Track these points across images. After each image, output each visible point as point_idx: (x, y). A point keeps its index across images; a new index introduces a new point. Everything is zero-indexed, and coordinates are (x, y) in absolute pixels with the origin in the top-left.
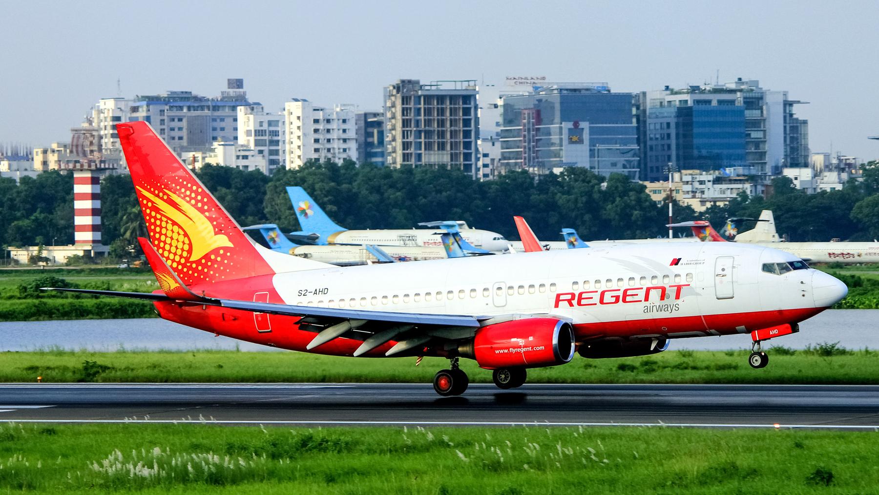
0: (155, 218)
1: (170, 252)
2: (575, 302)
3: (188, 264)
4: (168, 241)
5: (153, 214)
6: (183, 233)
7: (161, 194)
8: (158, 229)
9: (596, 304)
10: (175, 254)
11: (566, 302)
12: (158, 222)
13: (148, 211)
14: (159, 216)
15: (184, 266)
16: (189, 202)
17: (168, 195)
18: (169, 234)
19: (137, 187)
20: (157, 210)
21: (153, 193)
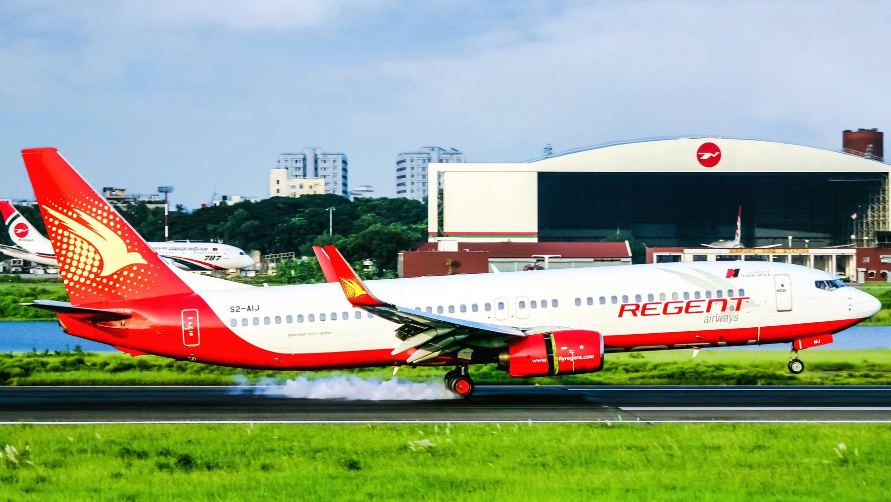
0: (62, 235)
1: (77, 267)
2: (638, 313)
3: (98, 279)
4: (76, 257)
5: (60, 231)
6: (94, 250)
7: (70, 213)
8: (64, 246)
9: (659, 314)
10: (83, 270)
11: (631, 312)
12: (65, 240)
13: (54, 229)
14: (66, 233)
15: (93, 281)
16: (101, 222)
17: (78, 214)
18: (78, 250)
19: (43, 206)
20: (65, 228)
21: (62, 212)
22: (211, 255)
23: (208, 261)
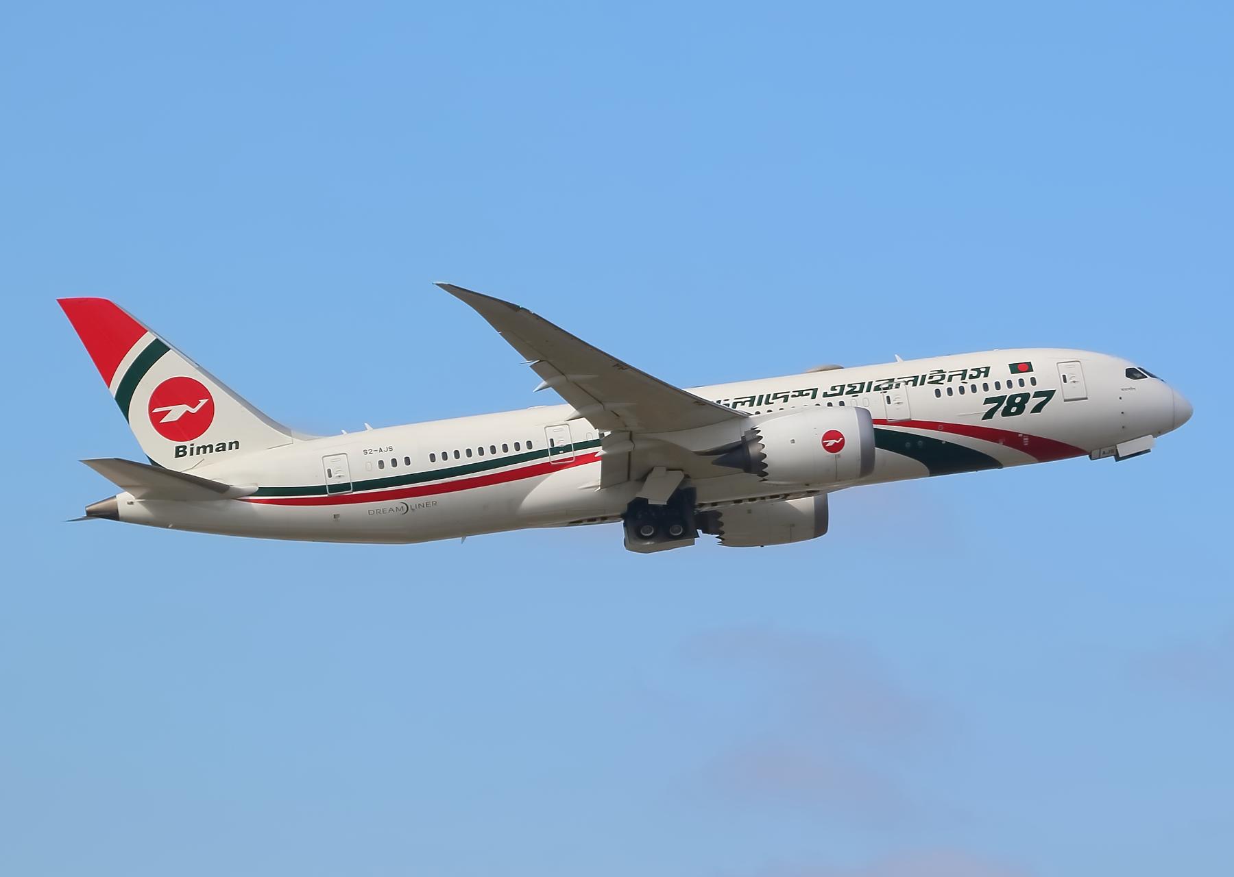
22: (1005, 392)
23: (999, 422)
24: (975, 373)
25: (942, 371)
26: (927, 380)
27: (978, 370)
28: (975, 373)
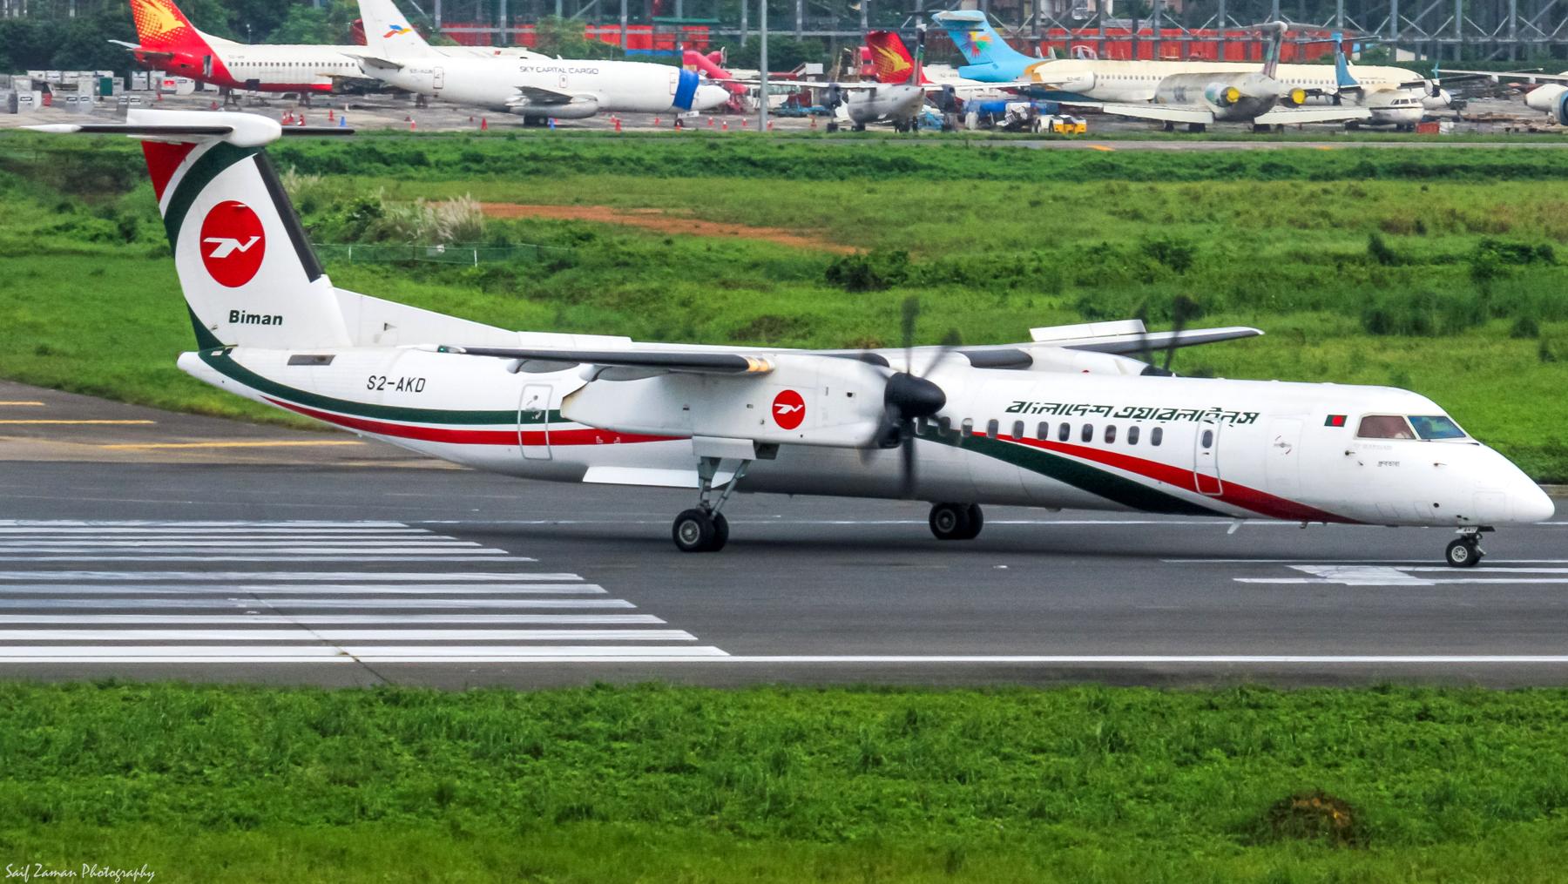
24: (1243, 417)
25: (1219, 410)
26: (1203, 416)
27: (1248, 415)
28: (1243, 417)
